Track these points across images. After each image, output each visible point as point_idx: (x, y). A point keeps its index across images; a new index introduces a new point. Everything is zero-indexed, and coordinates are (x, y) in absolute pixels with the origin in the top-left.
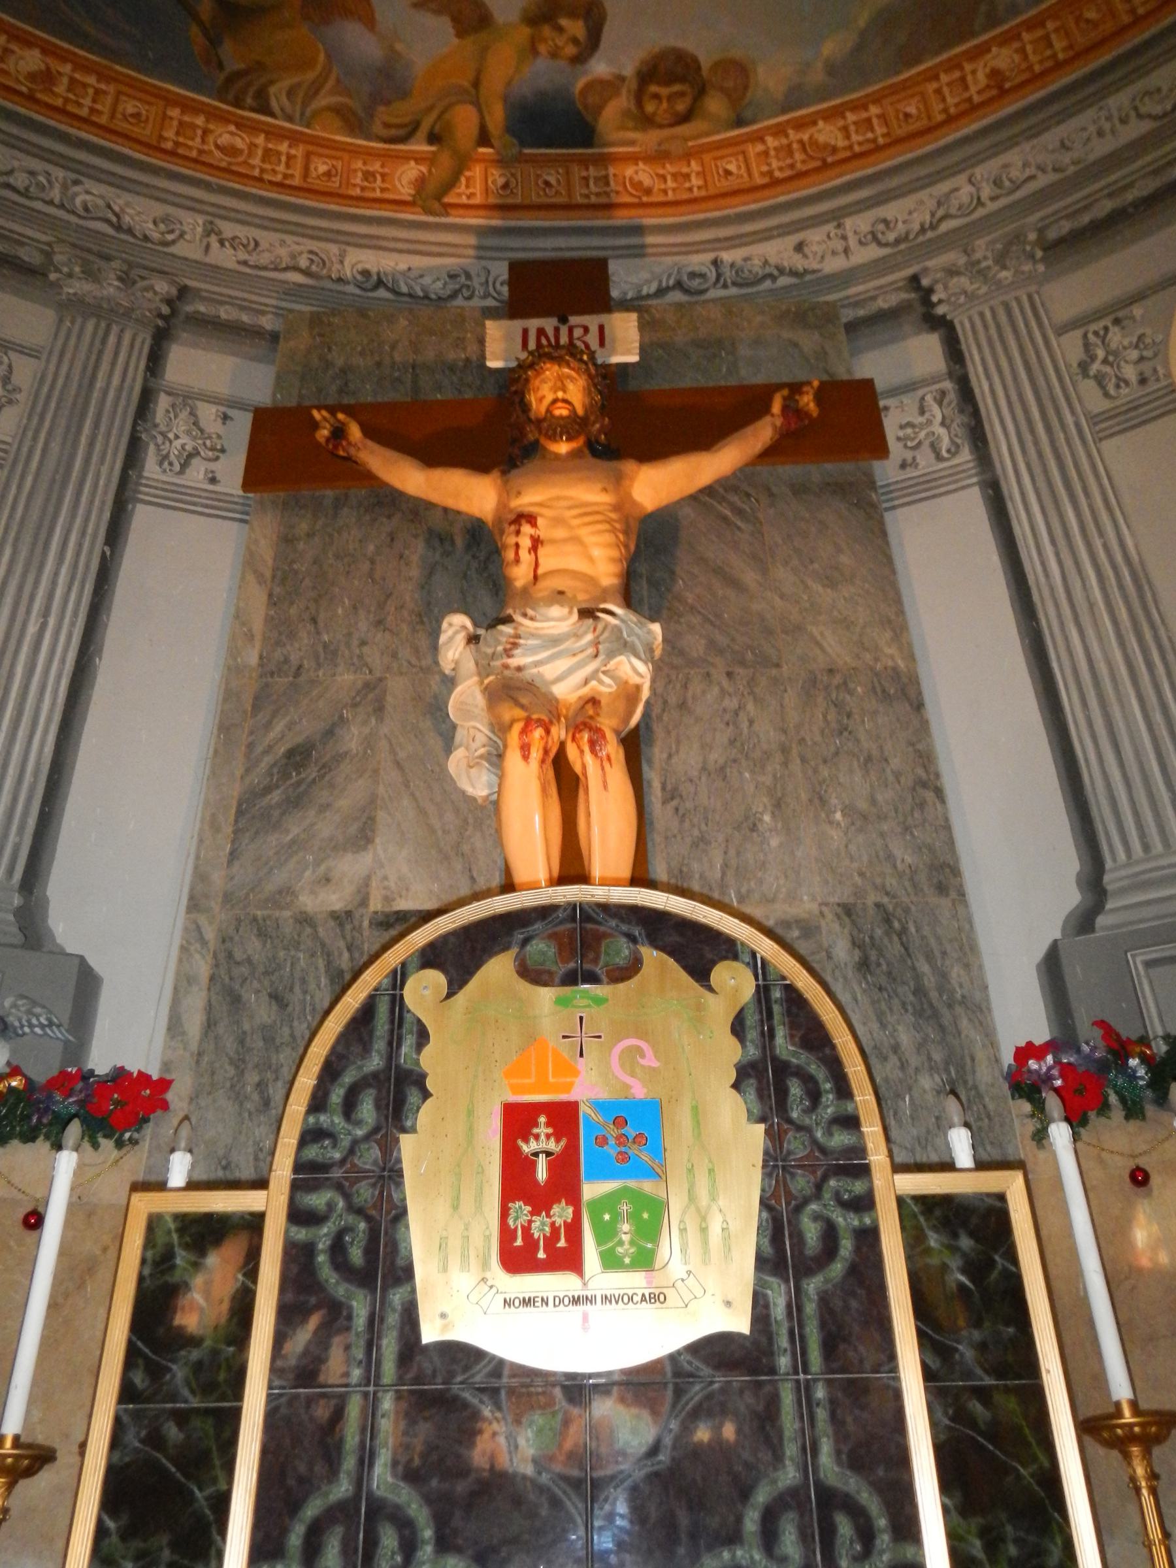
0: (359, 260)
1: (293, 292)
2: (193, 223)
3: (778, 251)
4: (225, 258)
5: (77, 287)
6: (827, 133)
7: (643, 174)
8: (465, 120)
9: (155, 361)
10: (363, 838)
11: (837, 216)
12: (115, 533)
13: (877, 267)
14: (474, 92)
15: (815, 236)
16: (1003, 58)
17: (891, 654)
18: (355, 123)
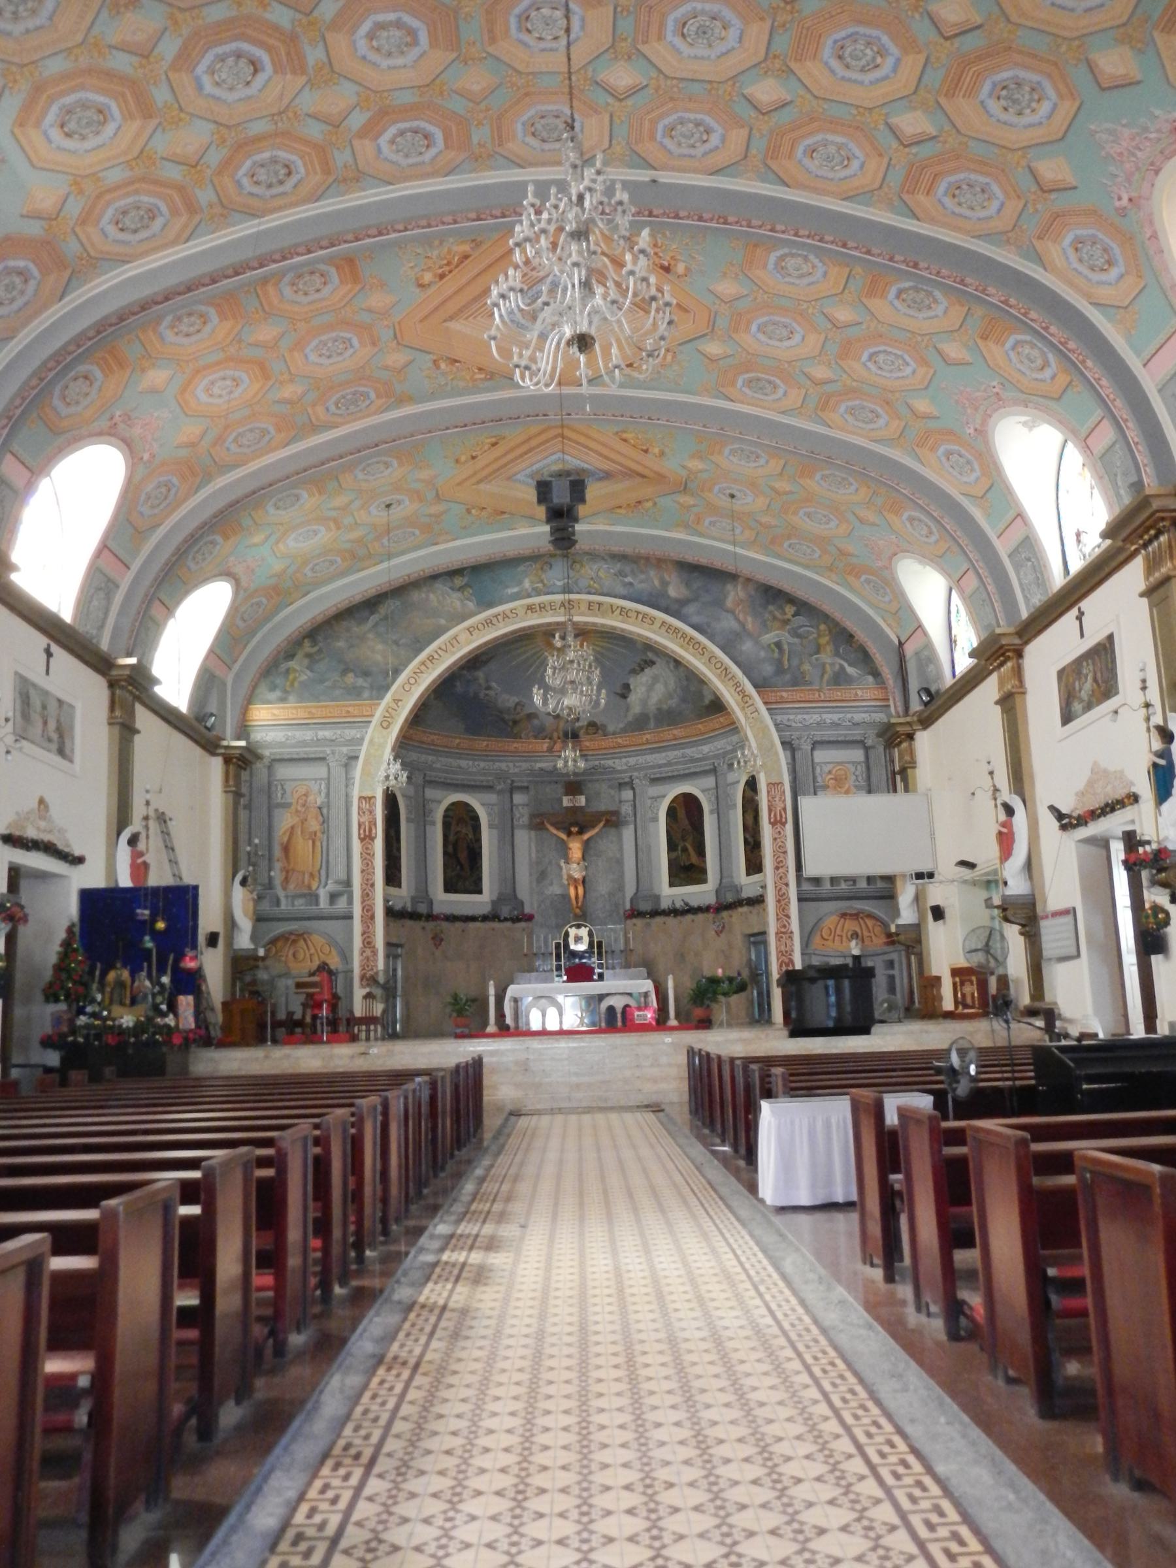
0: (539, 765)
1: (528, 775)
2: (511, 765)
3: (610, 763)
4: (516, 770)
5: (499, 788)
6: (620, 740)
7: (587, 744)
8: (555, 735)
9: (512, 798)
10: (551, 884)
11: (620, 758)
12: (513, 835)
13: (625, 771)
14: (557, 730)
15: (617, 761)
16: (648, 736)
17: (618, 856)
18: (536, 737)
